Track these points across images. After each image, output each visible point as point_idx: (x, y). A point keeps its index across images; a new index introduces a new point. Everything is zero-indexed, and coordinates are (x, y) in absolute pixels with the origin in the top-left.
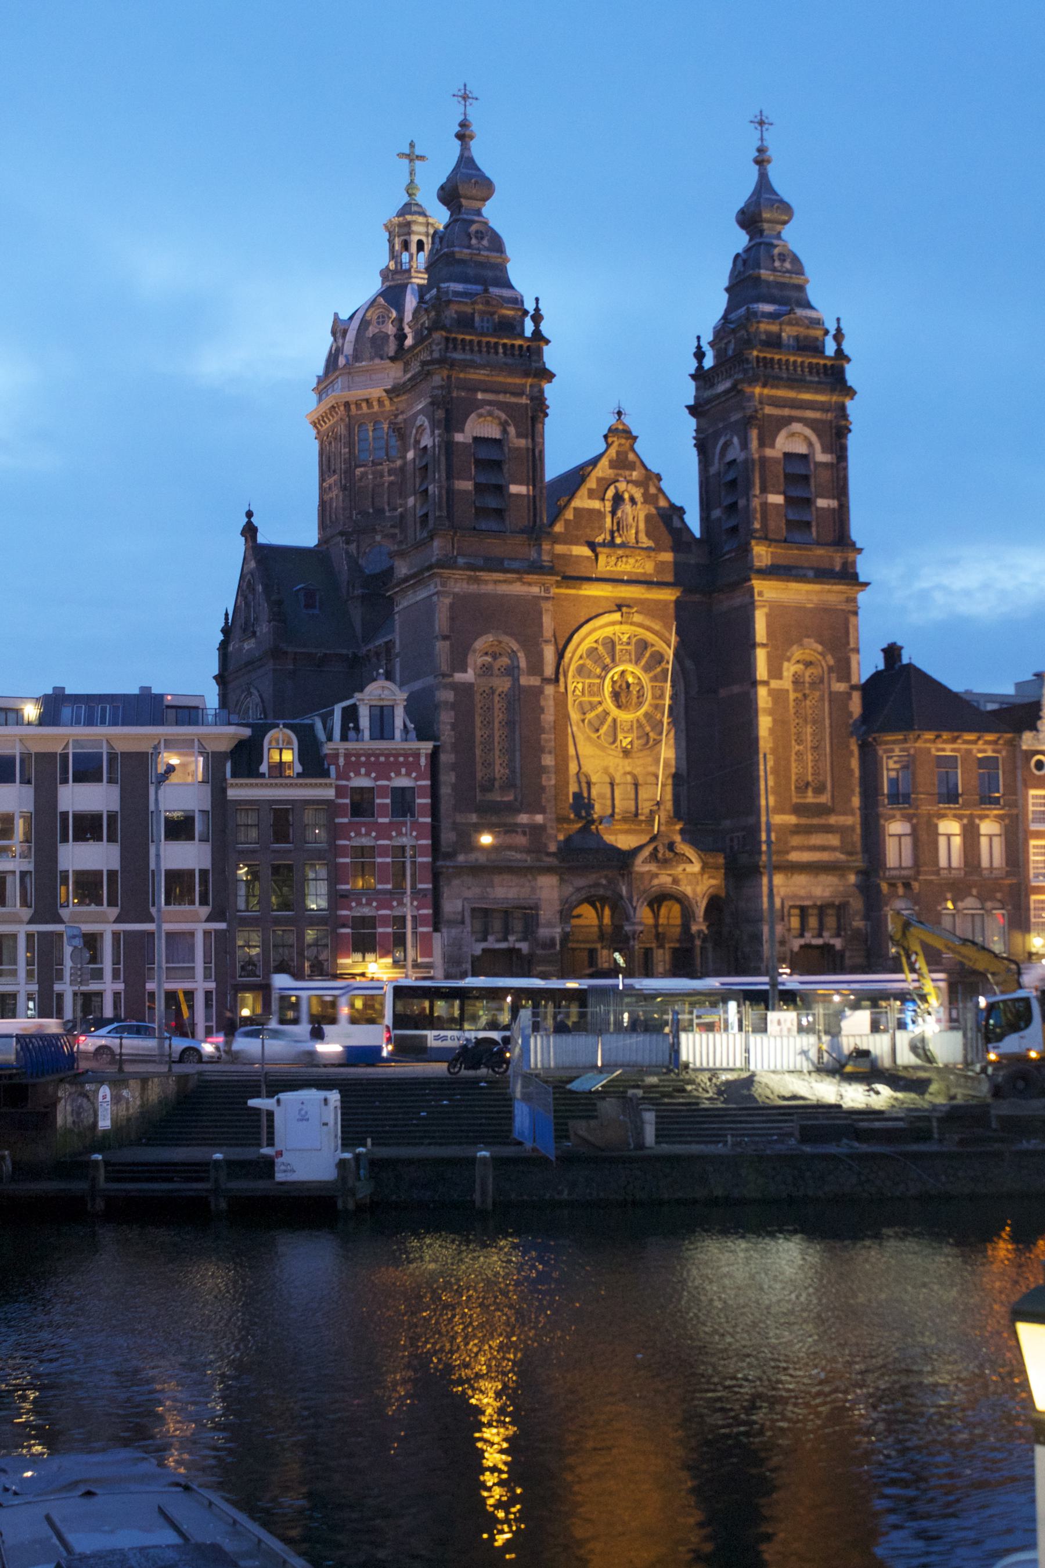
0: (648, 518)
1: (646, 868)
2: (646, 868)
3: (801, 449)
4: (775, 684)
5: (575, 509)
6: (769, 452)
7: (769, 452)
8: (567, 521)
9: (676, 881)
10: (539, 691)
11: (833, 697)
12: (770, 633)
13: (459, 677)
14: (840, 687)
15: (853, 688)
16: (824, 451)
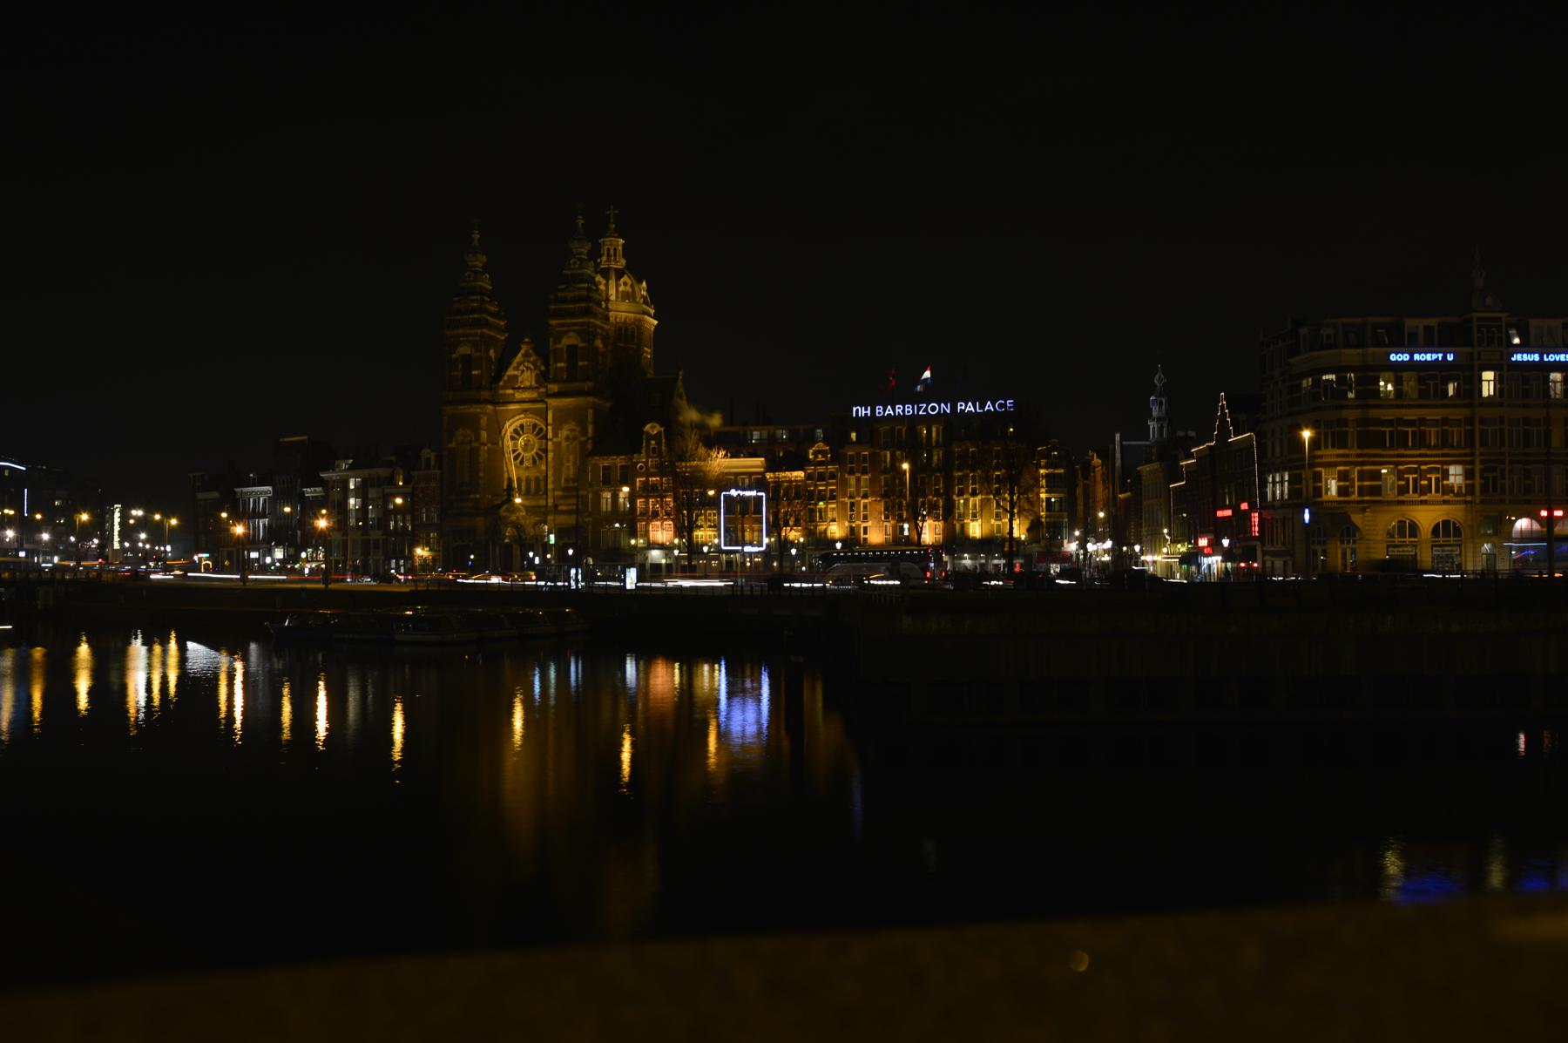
0: (536, 376)
1: (505, 514)
2: (505, 514)
3: (575, 342)
4: (555, 440)
5: (509, 376)
6: (558, 346)
7: (558, 346)
8: (505, 381)
9: (518, 519)
10: (478, 449)
11: (581, 443)
12: (553, 421)
13: (450, 445)
14: (584, 439)
15: (589, 439)
16: (582, 342)
